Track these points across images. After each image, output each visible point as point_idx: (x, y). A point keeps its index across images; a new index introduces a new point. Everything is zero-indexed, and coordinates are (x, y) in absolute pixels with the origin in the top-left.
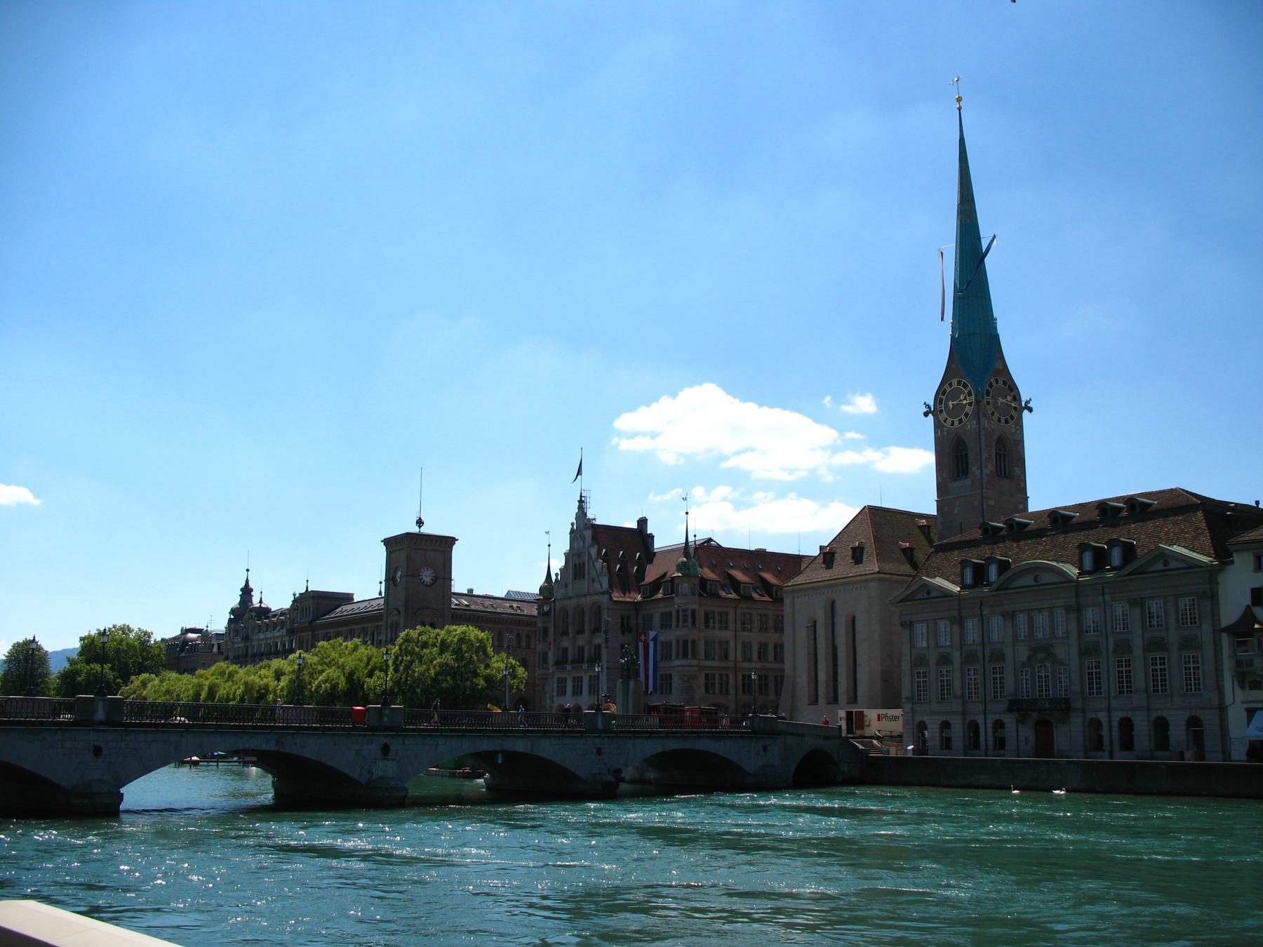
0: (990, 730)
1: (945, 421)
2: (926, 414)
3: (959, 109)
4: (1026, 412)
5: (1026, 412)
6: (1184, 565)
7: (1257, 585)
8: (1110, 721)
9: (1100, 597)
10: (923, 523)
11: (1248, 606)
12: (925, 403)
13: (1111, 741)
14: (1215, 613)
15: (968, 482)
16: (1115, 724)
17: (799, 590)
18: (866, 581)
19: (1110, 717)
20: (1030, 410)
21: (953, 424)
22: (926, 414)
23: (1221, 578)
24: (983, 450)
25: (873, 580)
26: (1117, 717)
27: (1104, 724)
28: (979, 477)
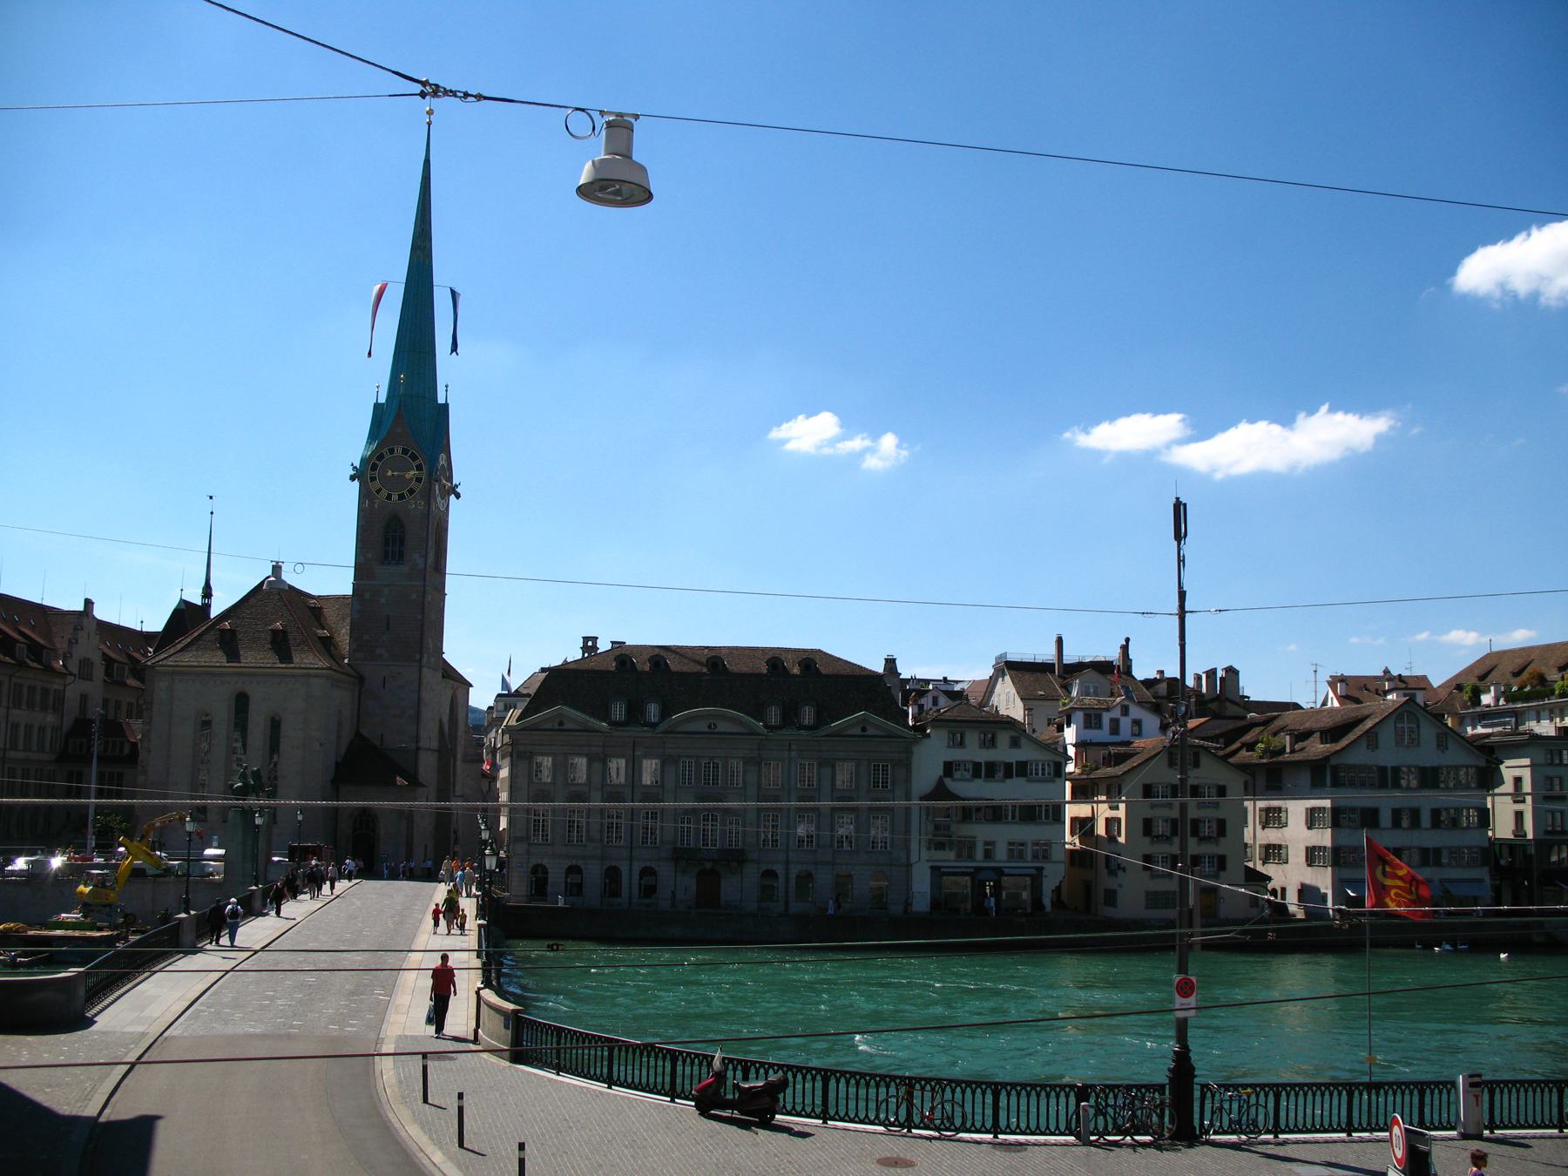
0: (636, 877)
1: (378, 491)
2: (352, 478)
3: (429, 124)
4: (452, 497)
5: (452, 497)
6: (884, 734)
7: (949, 759)
8: (787, 874)
9: (787, 753)
10: (314, 603)
11: (941, 777)
12: (352, 465)
13: (787, 892)
14: (908, 780)
15: (404, 569)
16: (793, 877)
17: (181, 673)
18: (309, 676)
19: (787, 869)
20: (458, 496)
21: (389, 497)
22: (352, 478)
23: (915, 749)
24: (430, 537)
25: (317, 676)
26: (795, 870)
27: (779, 875)
28: (421, 566)
